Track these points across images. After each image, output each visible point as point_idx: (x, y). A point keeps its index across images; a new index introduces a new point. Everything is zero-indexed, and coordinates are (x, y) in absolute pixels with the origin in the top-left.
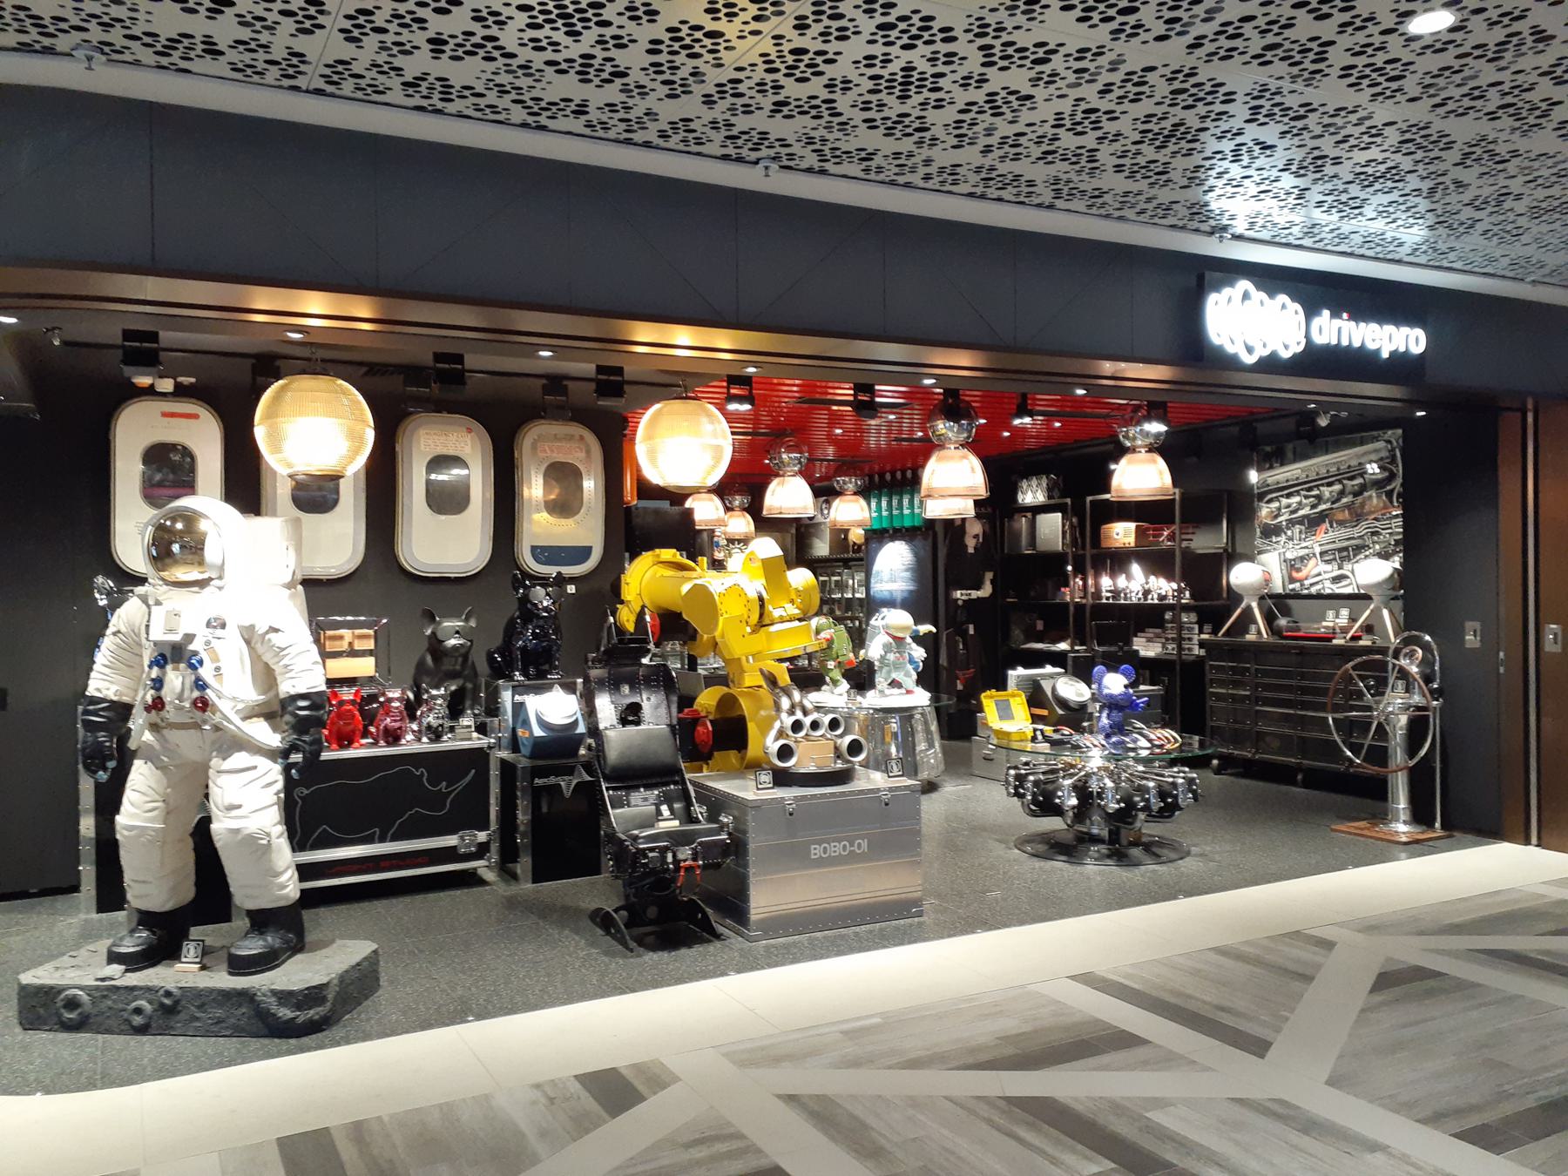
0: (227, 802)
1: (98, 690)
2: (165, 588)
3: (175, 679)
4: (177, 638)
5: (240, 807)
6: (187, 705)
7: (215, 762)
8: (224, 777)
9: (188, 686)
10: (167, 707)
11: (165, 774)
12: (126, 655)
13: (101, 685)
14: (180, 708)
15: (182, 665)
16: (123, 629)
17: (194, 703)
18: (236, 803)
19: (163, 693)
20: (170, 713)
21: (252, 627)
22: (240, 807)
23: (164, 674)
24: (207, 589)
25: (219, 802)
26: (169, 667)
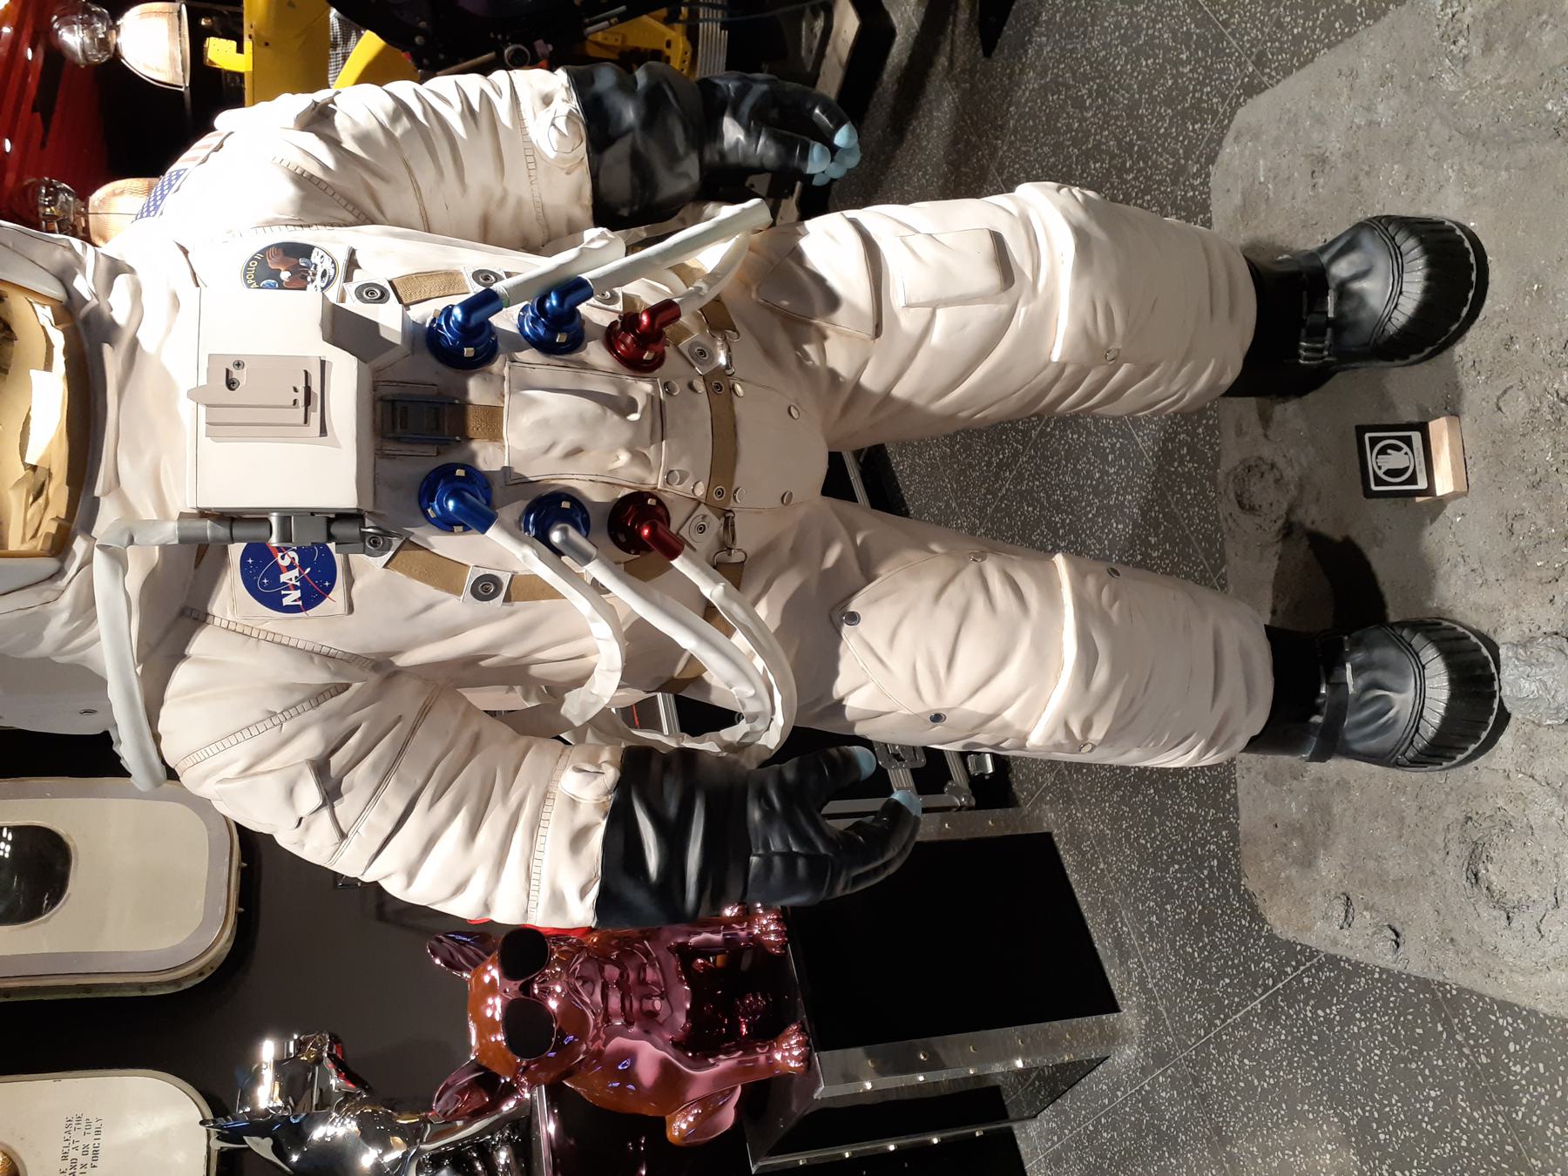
0: (984, 277)
1: (578, 838)
2: (108, 517)
3: (539, 425)
4: (345, 376)
5: (997, 238)
6: (642, 389)
7: (838, 355)
8: (897, 296)
9: (565, 377)
10: (655, 480)
11: (887, 554)
12: (427, 745)
13: (554, 837)
14: (660, 421)
15: (477, 391)
16: (310, 743)
17: (635, 364)
18: (988, 242)
19: (596, 495)
20: (674, 474)
21: (303, 181)
22: (997, 238)
23: (513, 481)
24: (119, 307)
25: (980, 315)
26: (488, 457)
